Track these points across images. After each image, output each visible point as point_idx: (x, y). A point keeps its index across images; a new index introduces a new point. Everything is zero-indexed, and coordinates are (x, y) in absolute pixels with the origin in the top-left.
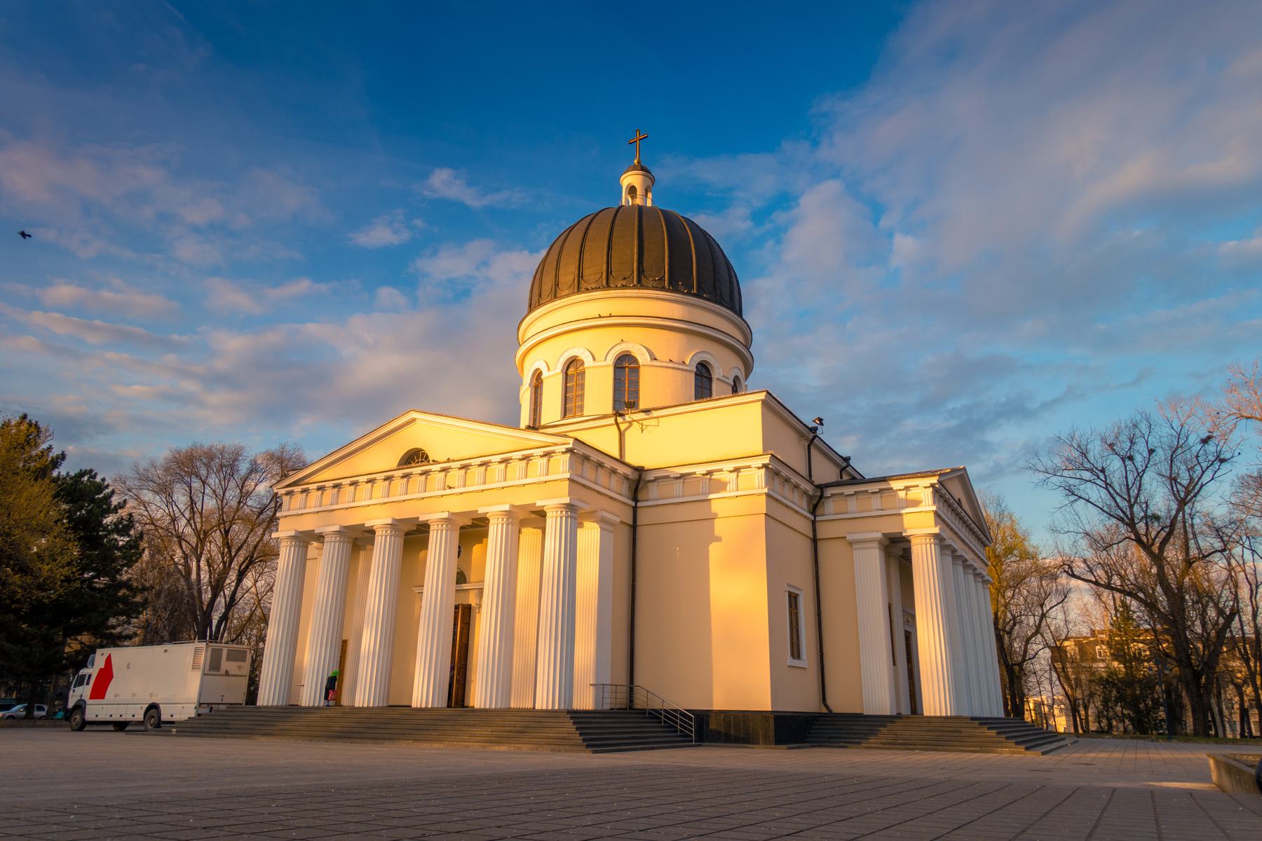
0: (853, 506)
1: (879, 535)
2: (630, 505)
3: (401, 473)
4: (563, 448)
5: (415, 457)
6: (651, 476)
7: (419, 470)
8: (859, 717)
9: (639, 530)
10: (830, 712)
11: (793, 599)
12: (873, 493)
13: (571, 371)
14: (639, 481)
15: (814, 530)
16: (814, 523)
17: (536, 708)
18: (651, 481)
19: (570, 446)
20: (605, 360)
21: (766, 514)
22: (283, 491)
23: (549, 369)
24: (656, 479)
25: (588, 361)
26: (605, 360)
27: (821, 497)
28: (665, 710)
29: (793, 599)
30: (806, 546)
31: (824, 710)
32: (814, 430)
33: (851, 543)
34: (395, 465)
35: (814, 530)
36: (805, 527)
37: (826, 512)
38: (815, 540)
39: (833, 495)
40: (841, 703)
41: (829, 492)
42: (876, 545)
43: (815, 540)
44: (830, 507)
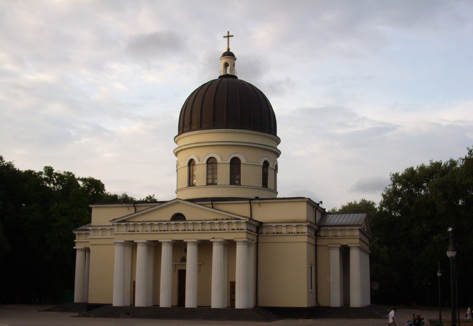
1: (339, 246)
2: (255, 235)
4: (244, 221)
5: (178, 217)
6: (264, 225)
7: (182, 222)
8: (329, 308)
9: (259, 245)
10: (319, 305)
11: (311, 267)
12: (338, 230)
13: (209, 162)
14: (259, 226)
17: (137, 305)
18: (264, 227)
19: (247, 221)
21: (307, 242)
22: (116, 224)
23: (199, 161)
24: (266, 226)
25: (219, 160)
29: (311, 267)
30: (313, 248)
31: (318, 305)
32: (318, 204)
33: (329, 248)
34: (169, 218)
35: (316, 242)
36: (314, 243)
38: (316, 246)
39: (324, 229)
41: (322, 228)
42: (338, 248)
44: (322, 234)
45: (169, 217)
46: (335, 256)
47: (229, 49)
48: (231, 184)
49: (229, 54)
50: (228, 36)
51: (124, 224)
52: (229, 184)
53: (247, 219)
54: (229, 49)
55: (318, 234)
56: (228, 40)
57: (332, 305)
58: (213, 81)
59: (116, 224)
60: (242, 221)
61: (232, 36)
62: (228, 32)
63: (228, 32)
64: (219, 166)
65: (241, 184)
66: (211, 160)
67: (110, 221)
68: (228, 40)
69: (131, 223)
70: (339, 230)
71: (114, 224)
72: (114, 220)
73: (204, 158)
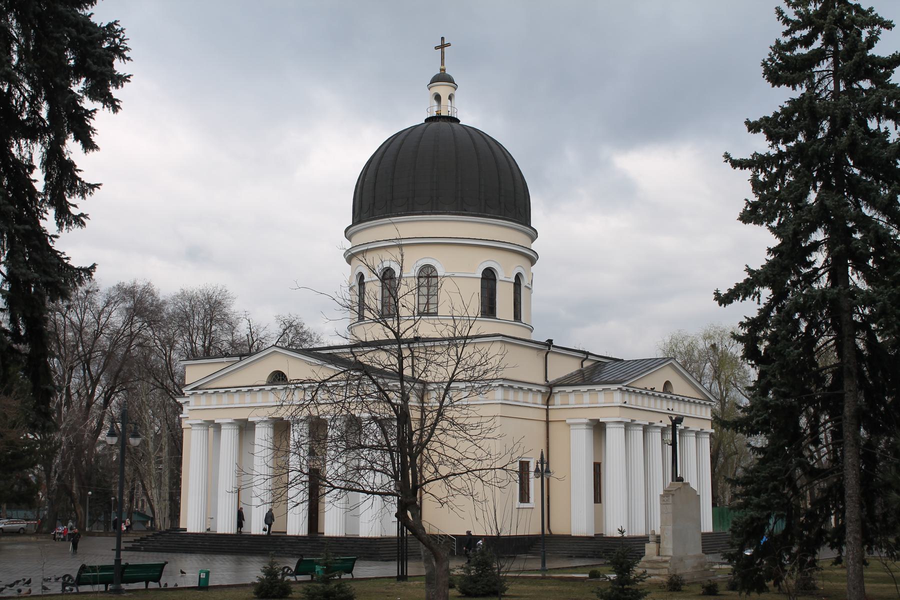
0: (572, 400)
3: (269, 388)
15: (547, 415)
16: (547, 410)
22: (190, 392)
27: (551, 393)
28: (440, 535)
30: (543, 425)
33: (569, 425)
35: (547, 415)
37: (556, 403)
38: (548, 422)
39: (559, 391)
40: (558, 528)
41: (556, 390)
43: (548, 422)
44: (558, 400)
45: (263, 378)
46: (581, 439)
47: (443, 70)
49: (442, 78)
50: (443, 46)
54: (443, 70)
55: (550, 403)
56: (443, 53)
57: (574, 533)
58: (413, 129)
59: (190, 392)
61: (449, 45)
62: (443, 39)
63: (443, 39)
66: (388, 273)
68: (443, 53)
70: (570, 392)
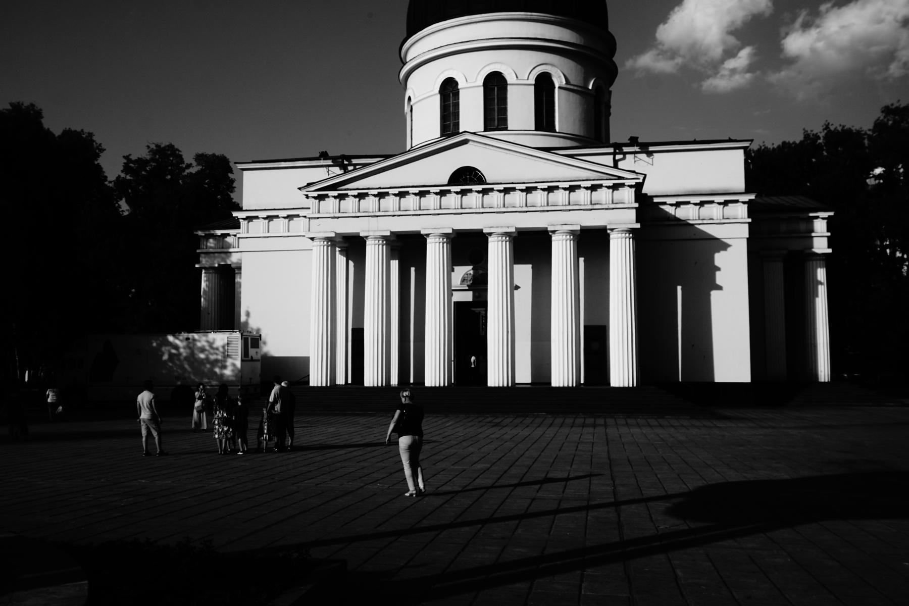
7: (480, 188)
20: (528, 79)
25: (510, 78)
26: (528, 79)
34: (446, 182)
48: (536, 129)
51: (335, 193)
52: (534, 129)
53: (639, 177)
59: (316, 194)
60: (627, 182)
64: (511, 91)
65: (555, 130)
67: (300, 189)
69: (350, 193)
71: (310, 194)
72: (309, 185)
73: (478, 74)
